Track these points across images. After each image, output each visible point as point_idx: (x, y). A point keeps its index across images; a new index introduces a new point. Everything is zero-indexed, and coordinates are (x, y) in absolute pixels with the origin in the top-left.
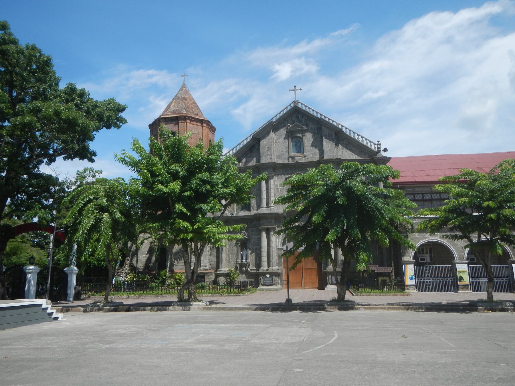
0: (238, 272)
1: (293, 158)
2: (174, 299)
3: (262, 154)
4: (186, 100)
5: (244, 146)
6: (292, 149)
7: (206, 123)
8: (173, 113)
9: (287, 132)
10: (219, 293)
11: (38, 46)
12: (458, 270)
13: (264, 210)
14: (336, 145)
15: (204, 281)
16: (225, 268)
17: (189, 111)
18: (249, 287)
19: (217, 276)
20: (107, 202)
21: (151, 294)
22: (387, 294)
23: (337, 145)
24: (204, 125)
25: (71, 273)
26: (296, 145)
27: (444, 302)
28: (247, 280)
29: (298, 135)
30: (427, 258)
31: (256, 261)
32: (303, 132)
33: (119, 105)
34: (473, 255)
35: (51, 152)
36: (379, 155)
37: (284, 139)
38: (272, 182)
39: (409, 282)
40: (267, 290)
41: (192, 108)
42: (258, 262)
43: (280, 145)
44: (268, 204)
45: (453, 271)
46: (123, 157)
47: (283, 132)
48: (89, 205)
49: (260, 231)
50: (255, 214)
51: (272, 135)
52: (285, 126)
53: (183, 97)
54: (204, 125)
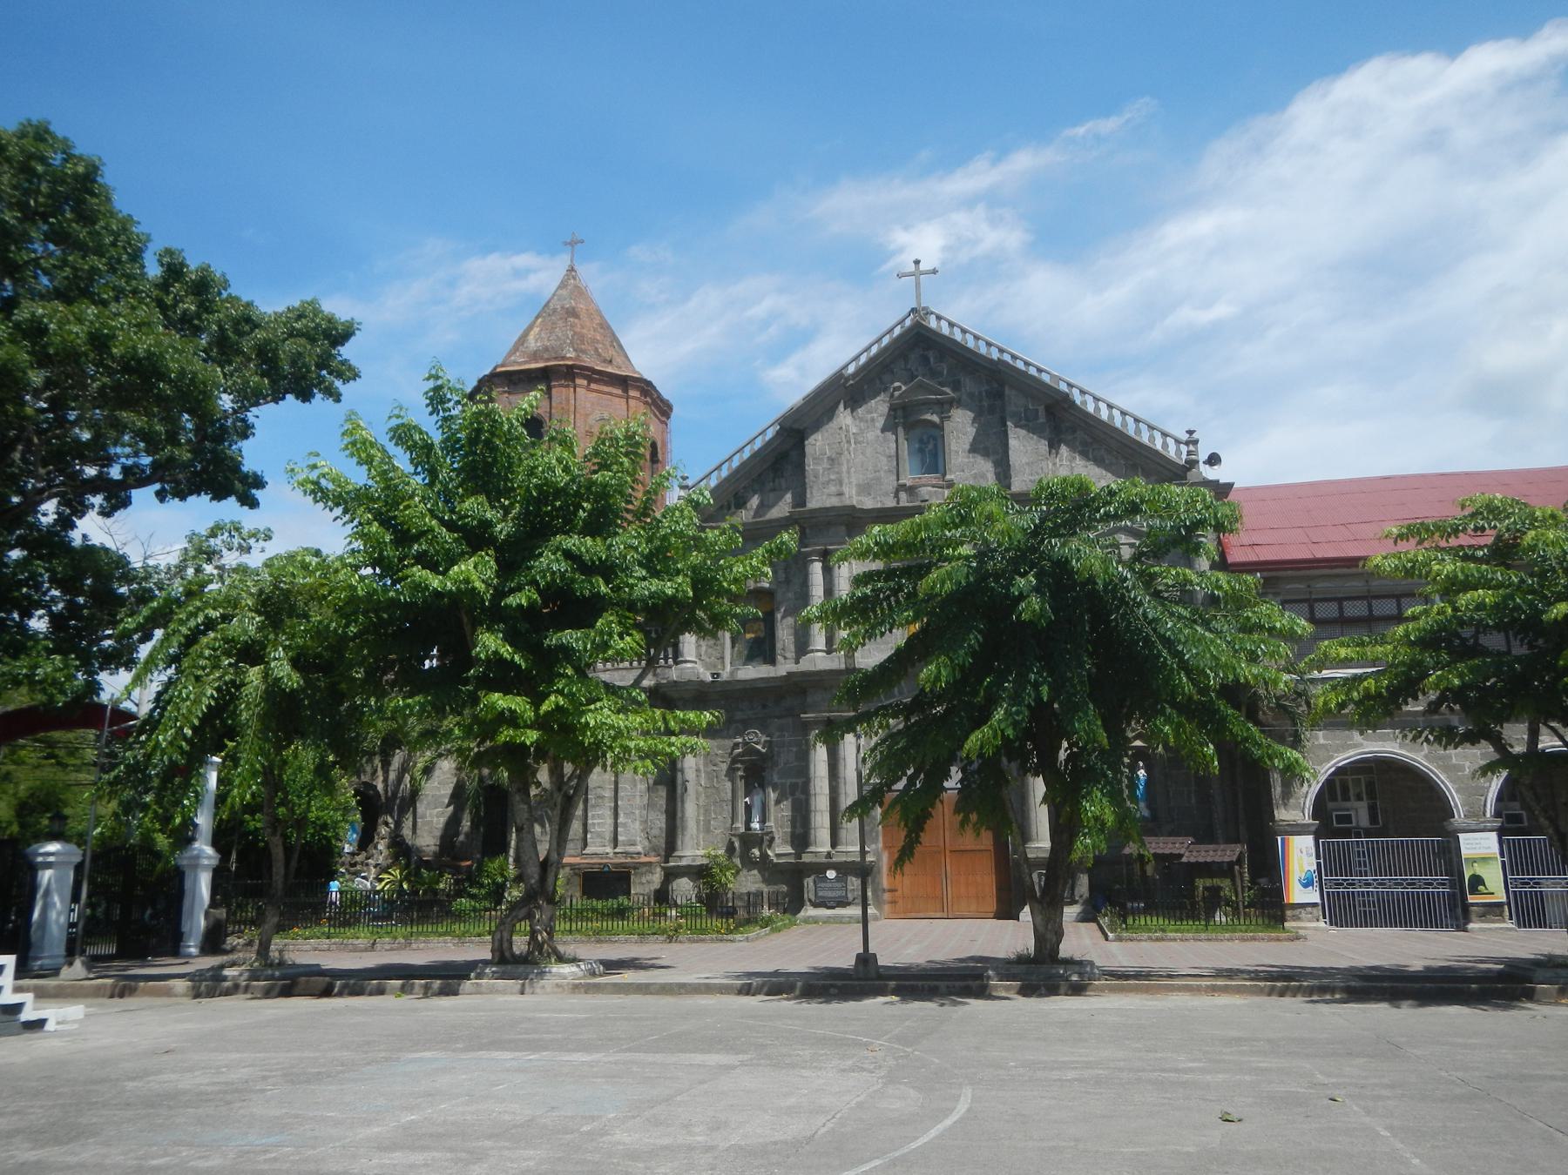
0: (737, 861)
1: (911, 490)
2: (480, 950)
3: (810, 478)
4: (577, 316)
5: (754, 456)
6: (906, 465)
7: (637, 388)
8: (535, 356)
9: (893, 409)
10: (664, 932)
11: (58, 129)
12: (1466, 851)
14: (1051, 446)
15: (628, 893)
16: (692, 851)
17: (584, 352)
18: (766, 912)
19: (671, 875)
20: (259, 629)
21: (445, 934)
22: (1220, 936)
23: (1053, 446)
24: (632, 393)
25: (196, 867)
26: (921, 451)
27: (1417, 965)
28: (766, 889)
29: (928, 417)
30: (1360, 813)
31: (793, 826)
32: (944, 407)
33: (330, 320)
34: (1517, 805)
35: (115, 473)
37: (883, 431)
39: (1297, 894)
40: (827, 920)
41: (594, 341)
42: (799, 831)
43: (869, 451)
45: (1449, 856)
46: (314, 476)
47: (878, 408)
48: (204, 640)
49: (806, 727)
50: (790, 674)
51: (844, 418)
52: (885, 390)
53: (567, 308)
54: (632, 393)
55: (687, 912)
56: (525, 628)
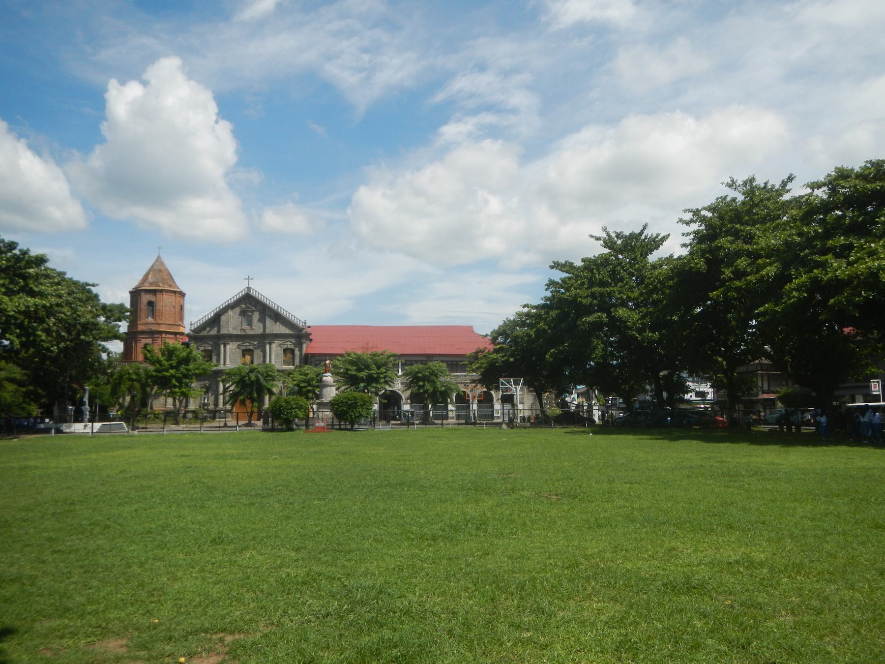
8: (151, 284)
13: (221, 367)
16: (192, 406)
23: (276, 322)
32: (253, 312)
36: (304, 331)
38: (228, 347)
44: (225, 362)
47: (238, 310)
51: (230, 312)
55: (190, 419)
56: (179, 380)
